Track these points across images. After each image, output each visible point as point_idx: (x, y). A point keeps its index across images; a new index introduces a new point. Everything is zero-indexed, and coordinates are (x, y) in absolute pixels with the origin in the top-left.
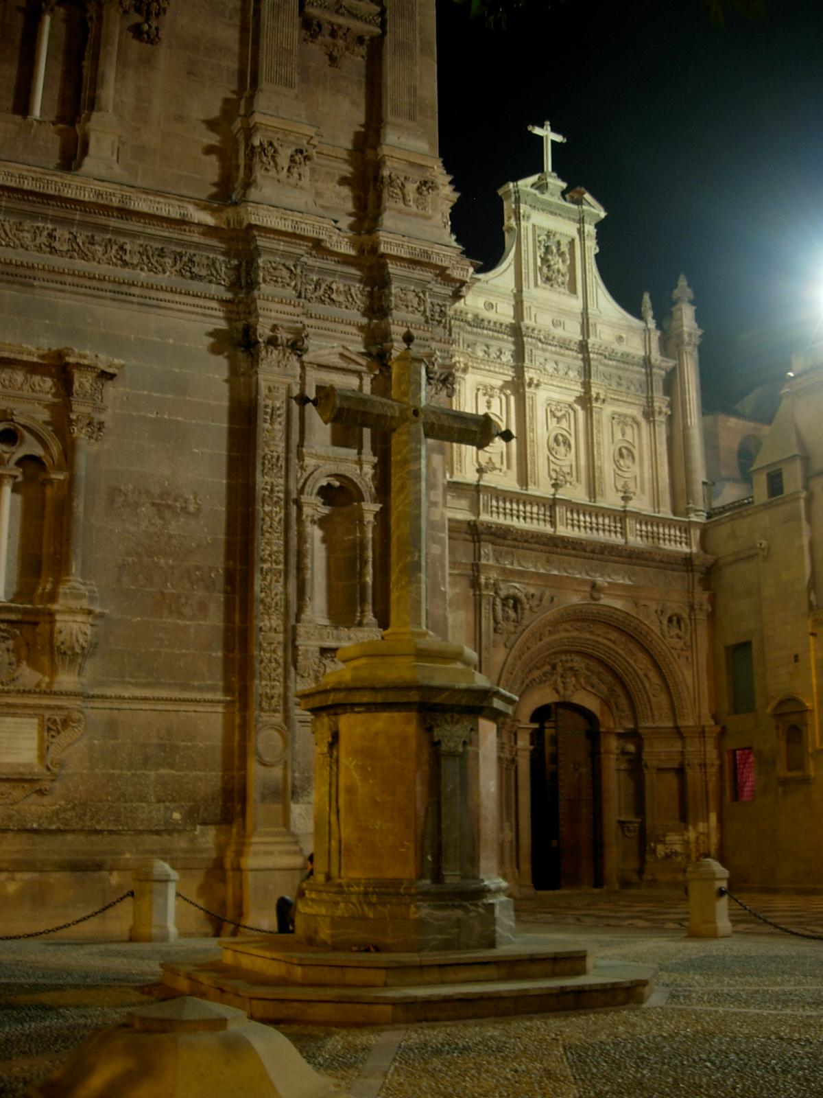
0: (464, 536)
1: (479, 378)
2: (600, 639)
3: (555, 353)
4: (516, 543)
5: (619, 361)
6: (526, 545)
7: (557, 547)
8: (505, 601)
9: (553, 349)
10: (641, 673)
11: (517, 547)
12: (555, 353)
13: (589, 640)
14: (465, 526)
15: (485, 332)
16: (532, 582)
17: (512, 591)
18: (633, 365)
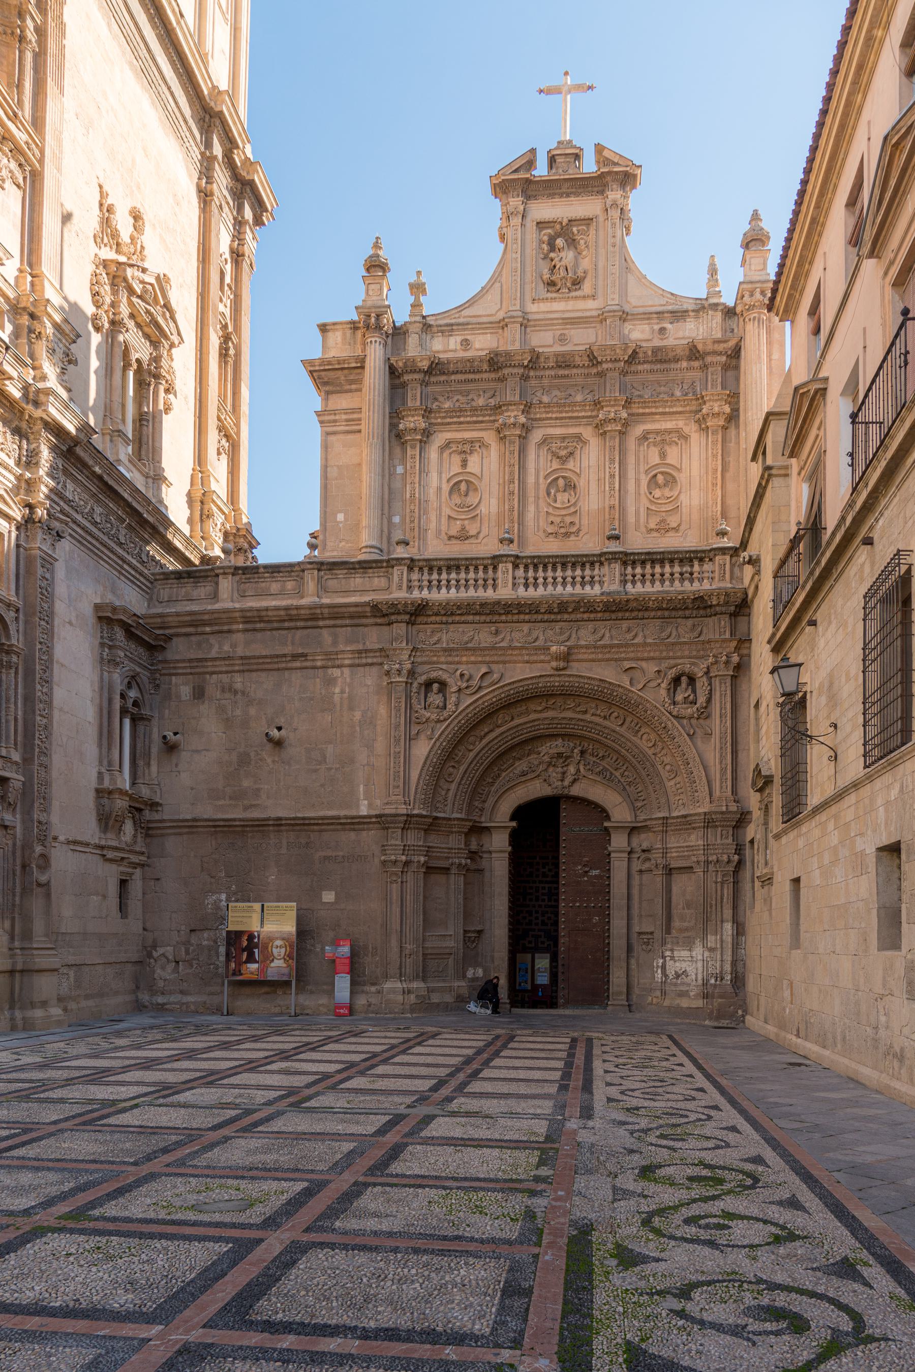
0: (371, 621)
1: (449, 435)
2: (588, 717)
3: (557, 377)
4: (444, 619)
5: (651, 362)
6: (457, 618)
7: (500, 614)
8: (428, 685)
9: (553, 373)
10: (650, 752)
11: (447, 623)
12: (557, 377)
13: (571, 719)
14: (368, 609)
15: (453, 377)
16: (464, 659)
17: (433, 675)
18: (677, 360)
